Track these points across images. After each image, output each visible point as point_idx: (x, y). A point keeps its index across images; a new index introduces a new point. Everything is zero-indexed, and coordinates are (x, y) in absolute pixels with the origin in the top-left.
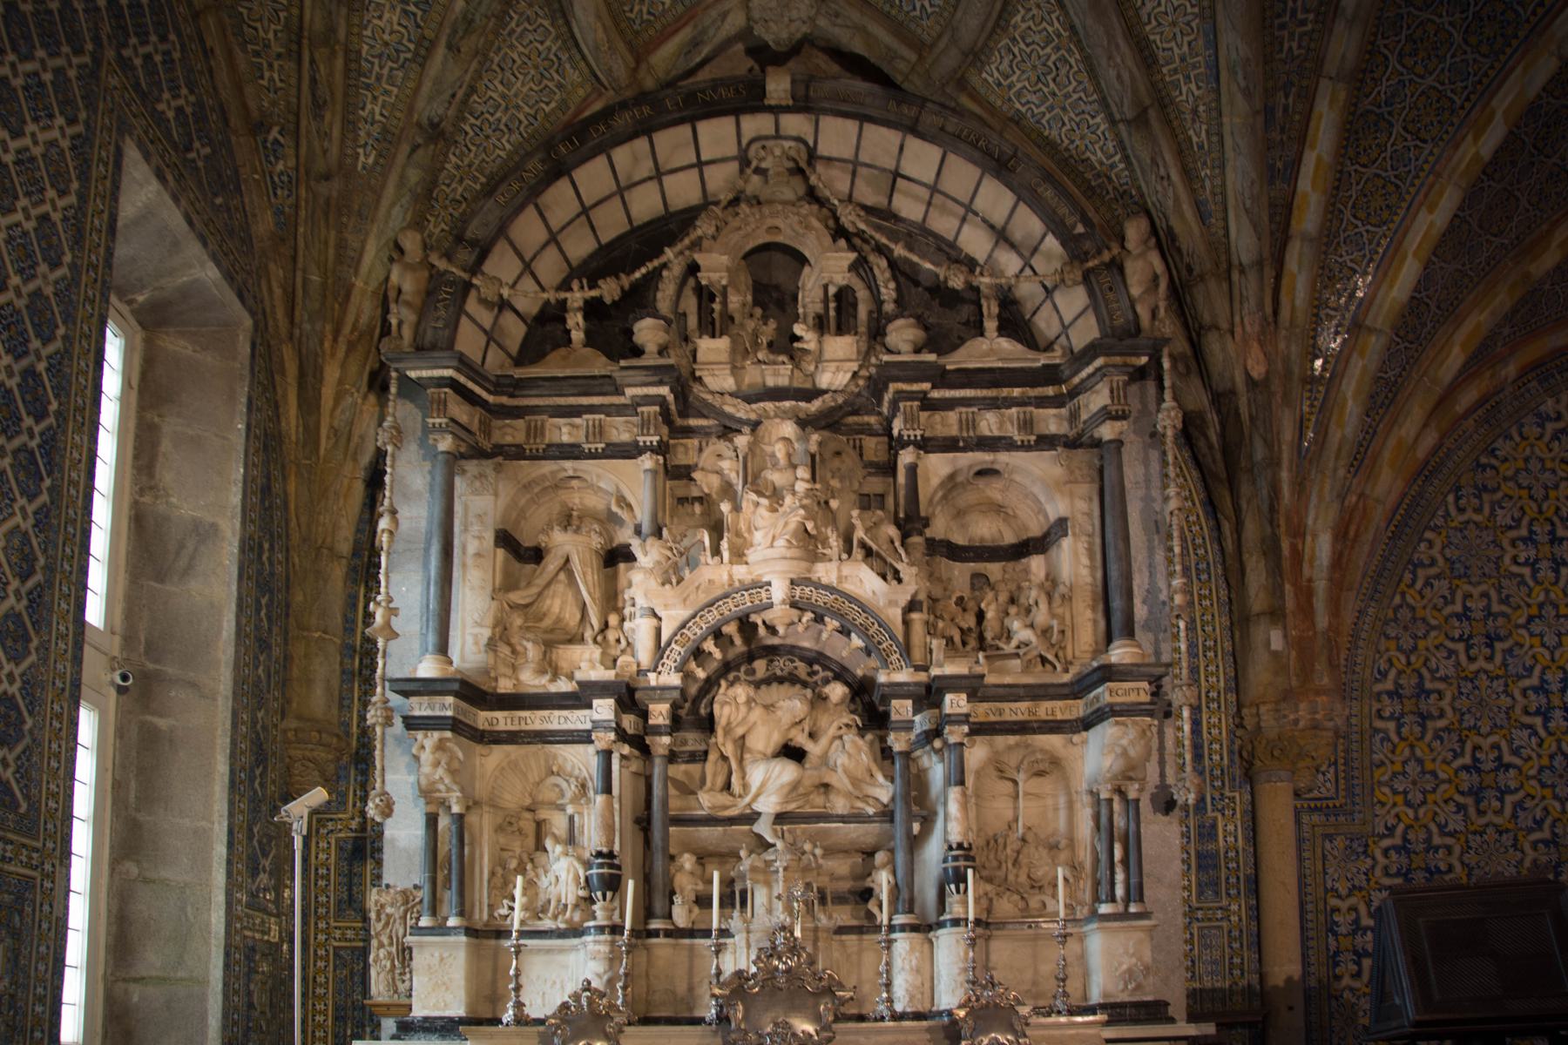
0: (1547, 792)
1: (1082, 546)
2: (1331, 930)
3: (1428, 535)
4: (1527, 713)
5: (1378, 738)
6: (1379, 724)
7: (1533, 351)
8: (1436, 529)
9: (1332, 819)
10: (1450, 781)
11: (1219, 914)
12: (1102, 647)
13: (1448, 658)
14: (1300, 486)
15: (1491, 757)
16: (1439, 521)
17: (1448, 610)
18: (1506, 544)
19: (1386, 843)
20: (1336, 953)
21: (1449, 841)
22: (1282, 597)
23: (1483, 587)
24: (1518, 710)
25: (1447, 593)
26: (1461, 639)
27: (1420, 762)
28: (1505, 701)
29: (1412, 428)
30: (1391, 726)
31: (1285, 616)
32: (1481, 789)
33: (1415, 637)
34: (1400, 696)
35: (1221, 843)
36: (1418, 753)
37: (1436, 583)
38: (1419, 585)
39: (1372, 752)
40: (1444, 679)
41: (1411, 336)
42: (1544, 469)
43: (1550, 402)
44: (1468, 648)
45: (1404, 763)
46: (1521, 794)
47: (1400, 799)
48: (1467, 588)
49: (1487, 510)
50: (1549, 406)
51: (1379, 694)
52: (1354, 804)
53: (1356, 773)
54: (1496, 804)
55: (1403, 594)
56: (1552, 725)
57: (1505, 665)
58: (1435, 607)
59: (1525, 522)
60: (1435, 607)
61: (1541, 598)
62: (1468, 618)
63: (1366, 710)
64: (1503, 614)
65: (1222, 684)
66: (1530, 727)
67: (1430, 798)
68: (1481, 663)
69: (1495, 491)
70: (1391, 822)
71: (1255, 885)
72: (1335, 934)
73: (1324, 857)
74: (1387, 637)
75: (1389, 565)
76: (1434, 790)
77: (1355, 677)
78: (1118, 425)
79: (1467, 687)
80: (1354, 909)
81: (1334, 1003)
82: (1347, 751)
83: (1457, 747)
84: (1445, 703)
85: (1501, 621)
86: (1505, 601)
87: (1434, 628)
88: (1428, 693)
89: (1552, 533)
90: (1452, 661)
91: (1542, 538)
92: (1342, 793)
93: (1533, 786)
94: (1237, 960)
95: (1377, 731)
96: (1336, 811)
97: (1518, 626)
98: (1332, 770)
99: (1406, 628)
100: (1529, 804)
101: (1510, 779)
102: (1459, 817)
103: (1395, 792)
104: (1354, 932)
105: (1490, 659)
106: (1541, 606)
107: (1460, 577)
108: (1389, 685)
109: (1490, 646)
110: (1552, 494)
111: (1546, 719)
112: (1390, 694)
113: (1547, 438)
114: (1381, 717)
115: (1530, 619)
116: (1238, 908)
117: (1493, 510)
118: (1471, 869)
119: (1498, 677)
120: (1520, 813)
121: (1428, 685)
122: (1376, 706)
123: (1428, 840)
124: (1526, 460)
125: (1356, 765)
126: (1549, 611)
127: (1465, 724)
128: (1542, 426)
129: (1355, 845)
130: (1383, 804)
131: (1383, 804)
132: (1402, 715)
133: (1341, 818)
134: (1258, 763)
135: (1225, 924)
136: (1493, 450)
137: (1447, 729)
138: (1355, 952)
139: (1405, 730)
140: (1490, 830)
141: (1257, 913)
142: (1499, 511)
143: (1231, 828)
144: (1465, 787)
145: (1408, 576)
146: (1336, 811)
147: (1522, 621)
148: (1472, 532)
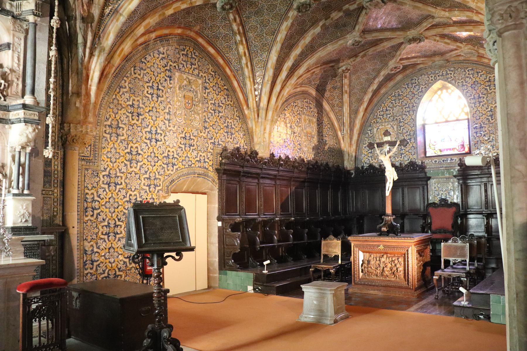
0: (149, 163)
1: (16, 55)
2: (85, 200)
3: (125, 78)
4: (146, 139)
5: (104, 139)
6: (105, 135)
7: (158, 33)
8: (127, 77)
9: (88, 163)
10: (123, 156)
11: (50, 193)
12: (20, 94)
13: (126, 118)
14: (91, 55)
15: (135, 150)
16: (129, 75)
17: (128, 103)
18: (146, 87)
19: (104, 173)
20: (87, 208)
21: (122, 175)
22: (81, 89)
23: (138, 98)
24: (144, 137)
25: (128, 98)
26: (130, 113)
27: (116, 149)
28: (140, 134)
29: (127, 47)
30: (108, 136)
31: (81, 96)
32: (132, 160)
33: (118, 109)
34: (112, 127)
35: (53, 168)
36: (115, 146)
37: (125, 94)
38: (121, 93)
39: (102, 144)
40: (125, 124)
41: (131, 19)
42: (158, 68)
43: (162, 48)
44: (132, 116)
45: (111, 148)
46: (142, 163)
47: (109, 160)
48: (134, 97)
49: (142, 76)
50: (161, 50)
51: (106, 125)
52: (95, 159)
53: (97, 150)
54: (135, 165)
55: (116, 95)
56: (152, 143)
57: (141, 123)
58: (124, 101)
59: (151, 82)
60: (124, 101)
61: (153, 105)
62: (133, 107)
63: (101, 130)
64: (143, 108)
65: (57, 113)
66: (146, 143)
67: (118, 161)
68: (135, 121)
69: (145, 70)
70: (106, 167)
71: (63, 184)
72: (87, 202)
73: (85, 176)
74: (110, 108)
75: (113, 85)
76: (119, 159)
77: (99, 119)
78: (36, 18)
79: (131, 128)
80: (92, 194)
81: (85, 224)
82: (95, 142)
83: (126, 146)
84: (124, 132)
85: (142, 110)
86: (144, 104)
87: (123, 108)
88: (120, 128)
89: (158, 87)
90: (127, 119)
91: (155, 88)
92: (92, 156)
93: (145, 161)
94: (55, 209)
95: (104, 137)
96: (90, 161)
97: (146, 112)
98: (89, 147)
99: (115, 106)
100: (144, 166)
101: (140, 158)
102: (125, 168)
103: (108, 158)
104: (92, 202)
105: (138, 120)
106: (153, 107)
107: (132, 94)
108: (109, 123)
109: (138, 117)
110: (159, 75)
111: (151, 141)
112: (109, 126)
113: (160, 59)
114: (105, 133)
115: (150, 111)
116: (57, 191)
117: (143, 76)
118: (127, 184)
119: (139, 126)
120: (142, 169)
121: (120, 125)
122: (104, 129)
123: (116, 174)
124: (154, 63)
125: (97, 147)
126: (154, 110)
127: (129, 139)
128: (159, 55)
129: (94, 173)
130: (104, 161)
131: (104, 161)
132: (112, 133)
133: (91, 164)
134: (68, 142)
135: (52, 196)
136: (146, 58)
137: (124, 140)
138: (92, 208)
139: (112, 138)
140: (133, 173)
141: (63, 193)
142: (145, 77)
143: (56, 163)
144: (127, 159)
145: (118, 90)
146: (90, 161)
147: (147, 111)
148: (137, 80)
